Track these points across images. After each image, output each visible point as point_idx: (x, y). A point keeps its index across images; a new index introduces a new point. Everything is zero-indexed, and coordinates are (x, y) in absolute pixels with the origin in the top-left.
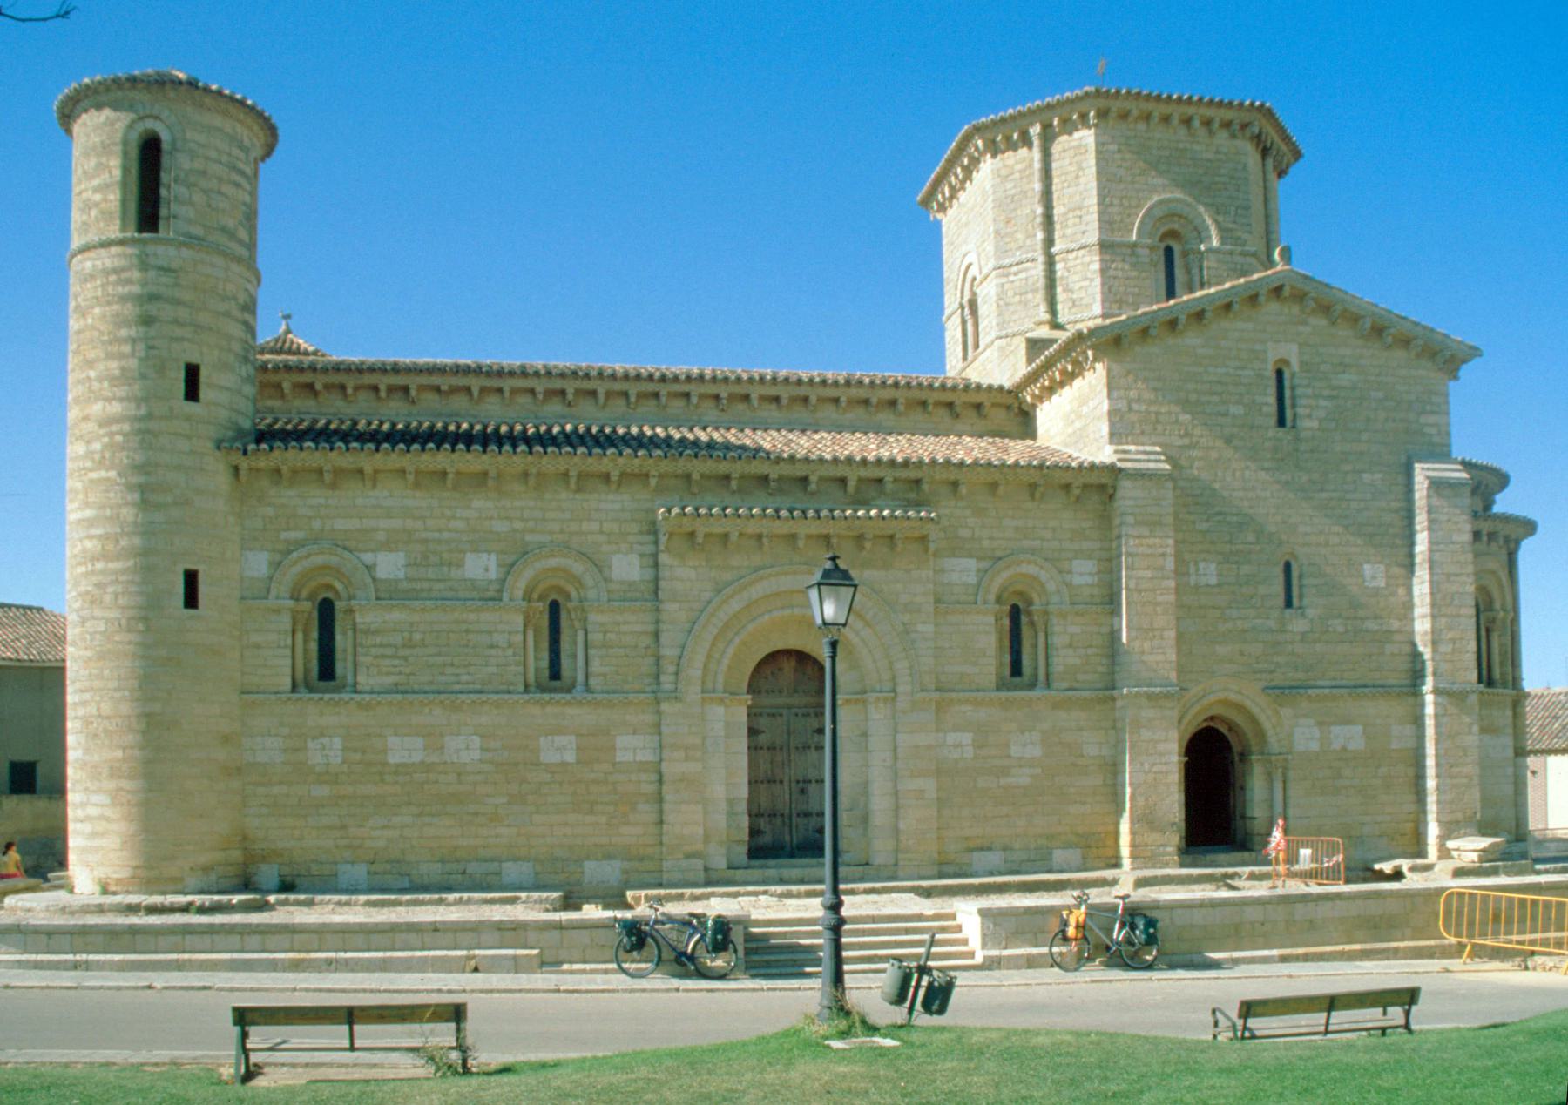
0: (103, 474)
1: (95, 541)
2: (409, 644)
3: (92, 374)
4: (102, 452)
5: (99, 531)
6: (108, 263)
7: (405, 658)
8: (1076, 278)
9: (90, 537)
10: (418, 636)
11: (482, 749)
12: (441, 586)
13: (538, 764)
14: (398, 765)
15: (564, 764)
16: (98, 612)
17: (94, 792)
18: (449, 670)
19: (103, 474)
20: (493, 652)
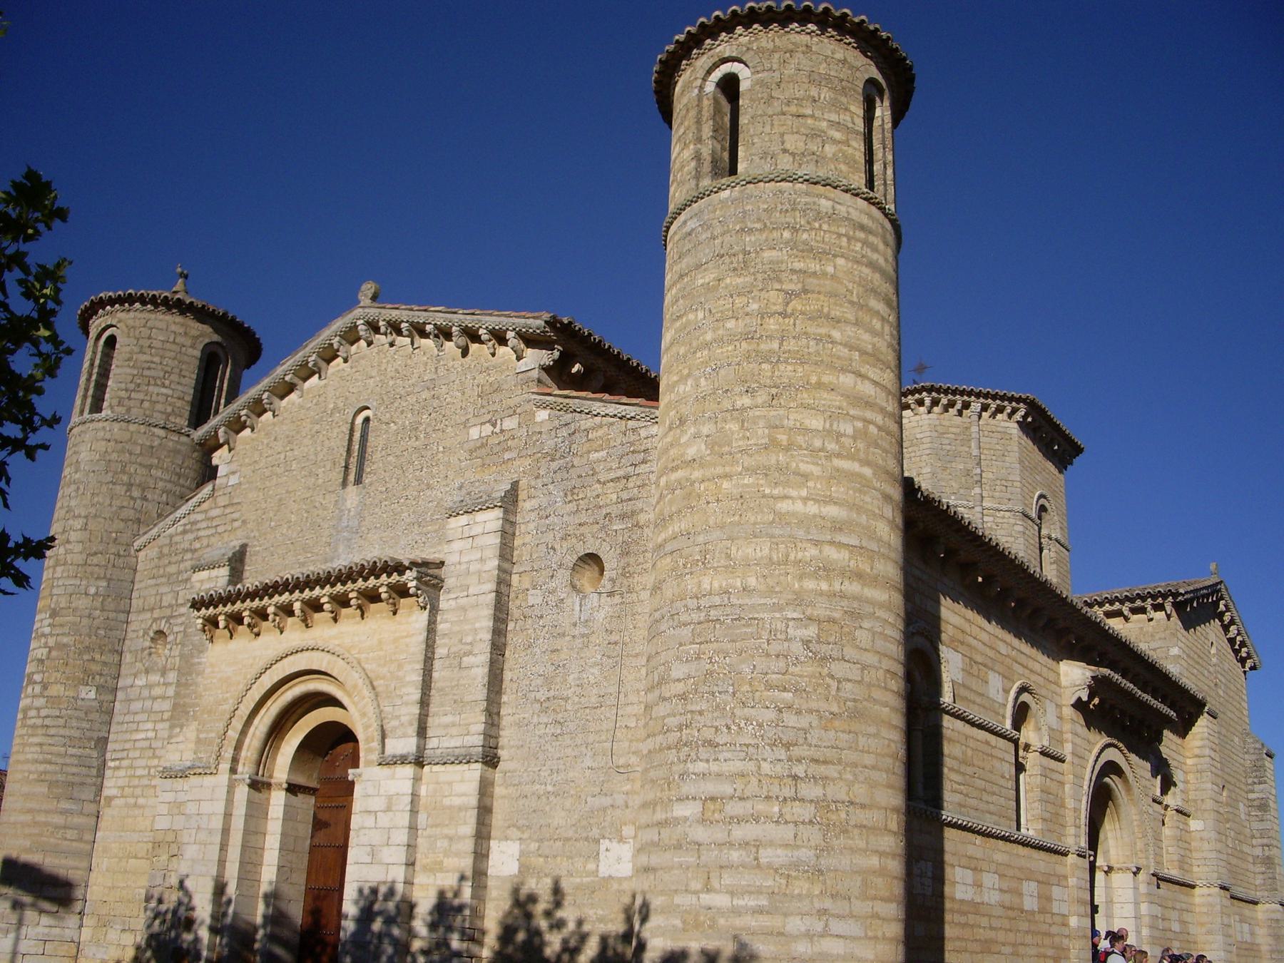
0: (854, 466)
1: (845, 554)
2: (964, 762)
3: (836, 335)
4: (854, 438)
5: (853, 541)
6: (855, 215)
7: (964, 774)
8: (1003, 532)
9: (840, 545)
10: (970, 752)
11: (1001, 890)
12: (978, 700)
13: (1022, 911)
14: (962, 901)
15: (1032, 913)
16: (849, 652)
17: (839, 917)
18: (985, 797)
19: (854, 466)
20: (1002, 782)
